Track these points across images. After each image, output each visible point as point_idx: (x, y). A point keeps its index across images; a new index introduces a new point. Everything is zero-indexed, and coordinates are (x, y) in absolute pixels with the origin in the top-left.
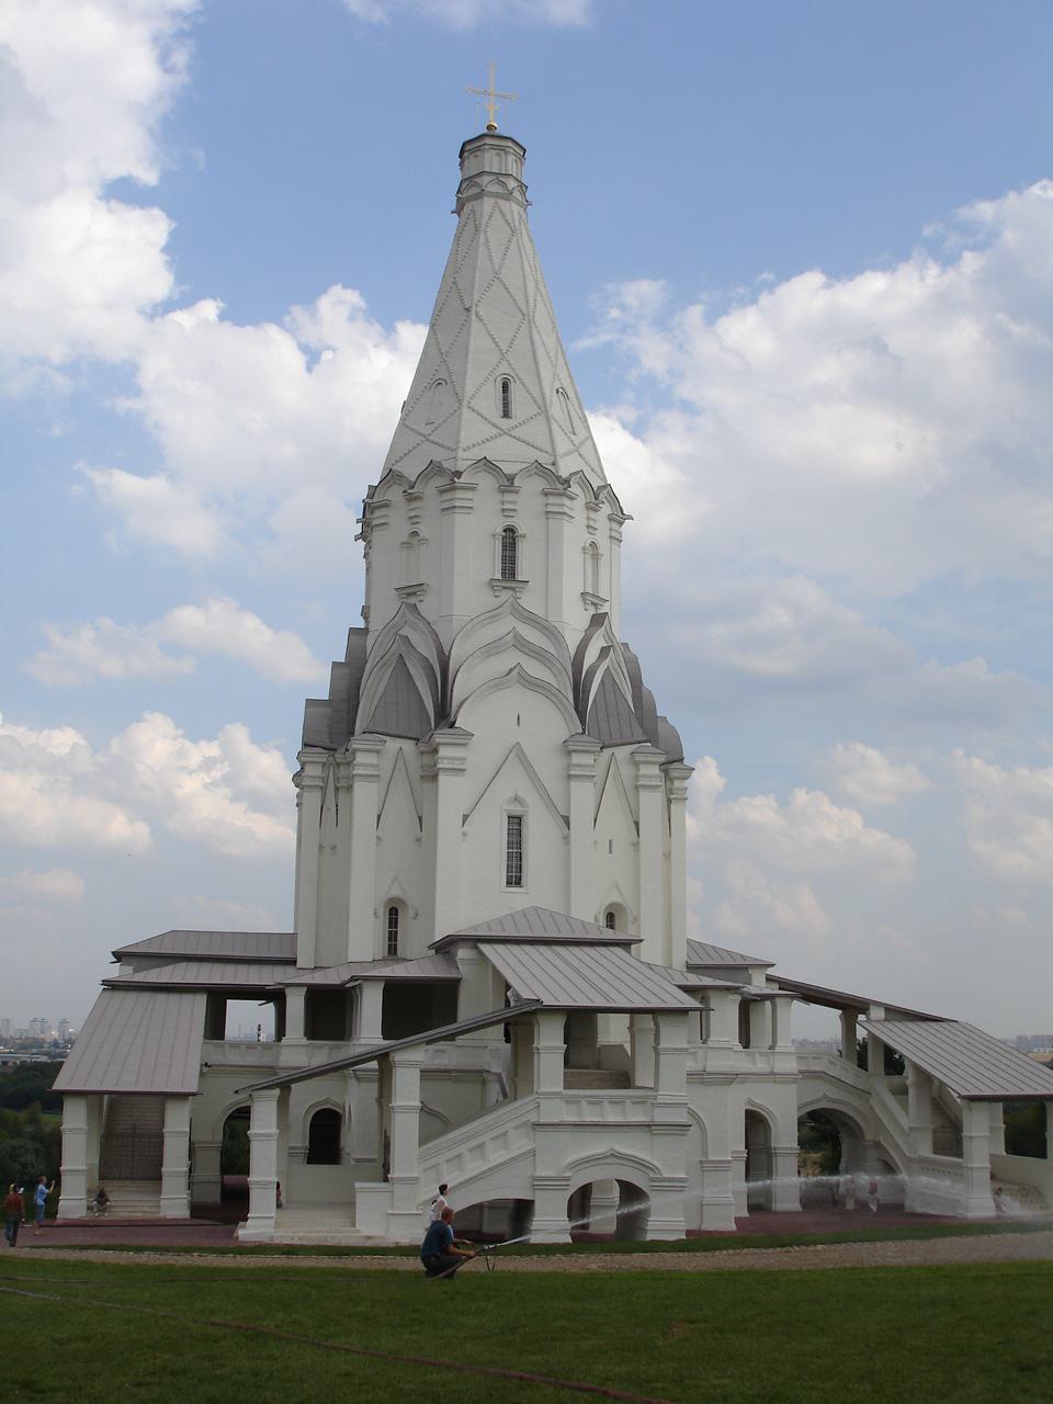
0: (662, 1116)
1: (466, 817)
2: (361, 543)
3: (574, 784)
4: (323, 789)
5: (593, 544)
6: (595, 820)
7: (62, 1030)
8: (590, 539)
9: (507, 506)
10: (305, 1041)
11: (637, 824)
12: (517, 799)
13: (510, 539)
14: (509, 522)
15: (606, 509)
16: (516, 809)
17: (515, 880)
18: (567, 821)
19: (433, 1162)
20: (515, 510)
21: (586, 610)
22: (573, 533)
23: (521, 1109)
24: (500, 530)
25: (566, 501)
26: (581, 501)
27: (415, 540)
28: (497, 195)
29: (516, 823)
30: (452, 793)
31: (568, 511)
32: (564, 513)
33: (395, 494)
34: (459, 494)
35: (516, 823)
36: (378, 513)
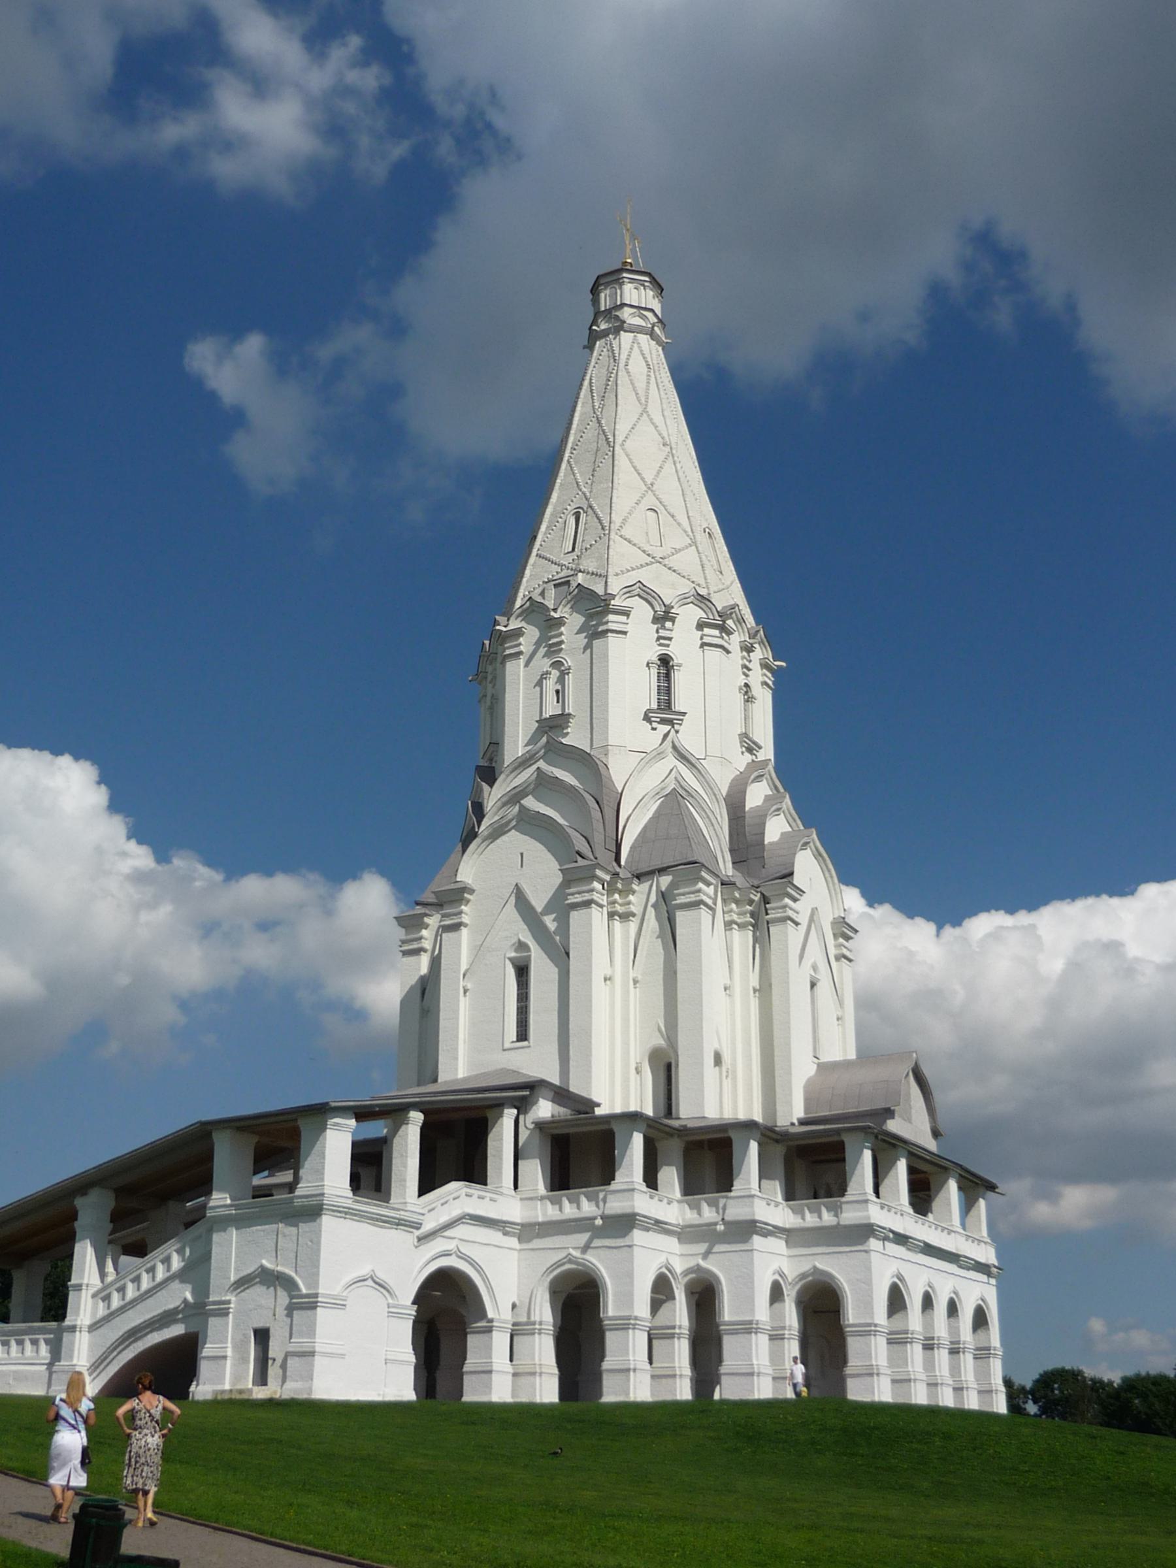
5: (665, 661)
12: (522, 946)
15: (688, 615)
25: (611, 617)
26: (642, 612)
29: (522, 972)
31: (611, 626)
35: (522, 972)
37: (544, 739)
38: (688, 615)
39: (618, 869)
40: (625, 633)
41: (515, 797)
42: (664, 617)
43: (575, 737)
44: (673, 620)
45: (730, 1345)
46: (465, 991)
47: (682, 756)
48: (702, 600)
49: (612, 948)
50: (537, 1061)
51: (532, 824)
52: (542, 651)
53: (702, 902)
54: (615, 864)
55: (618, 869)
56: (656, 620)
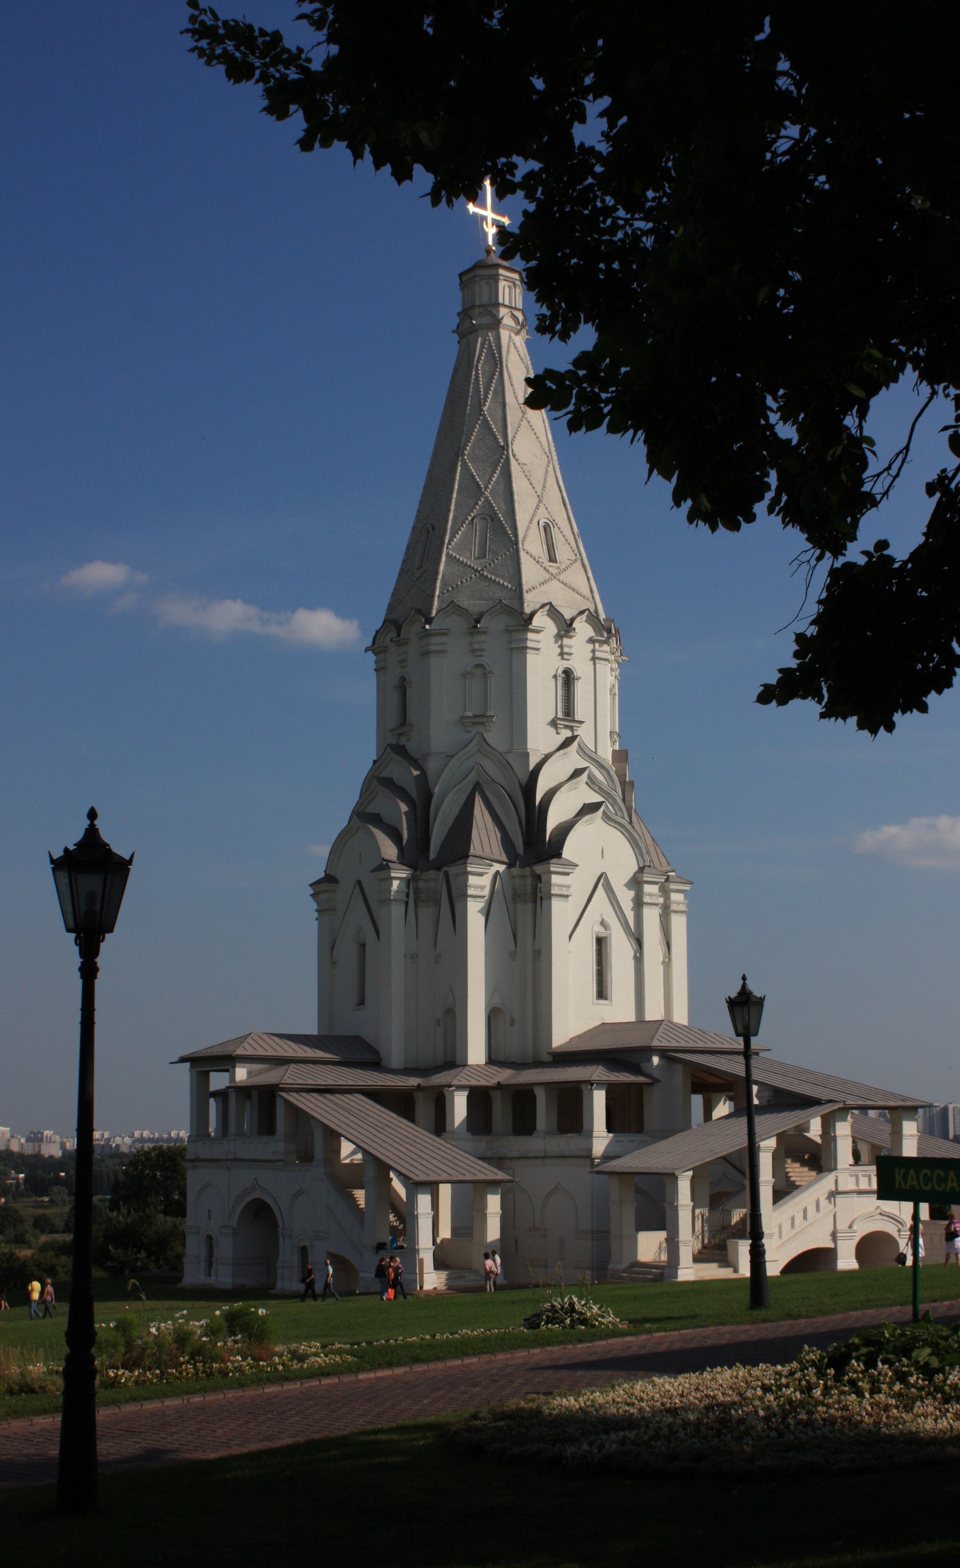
1: (570, 937)
2: (371, 657)
4: (407, 904)
9: (566, 650)
10: (469, 1135)
12: (603, 923)
13: (568, 678)
14: (566, 664)
17: (602, 993)
20: (570, 654)
23: (827, 1182)
24: (560, 671)
27: (479, 672)
28: (510, 329)
30: (561, 914)
33: (457, 624)
34: (530, 636)
36: (434, 640)
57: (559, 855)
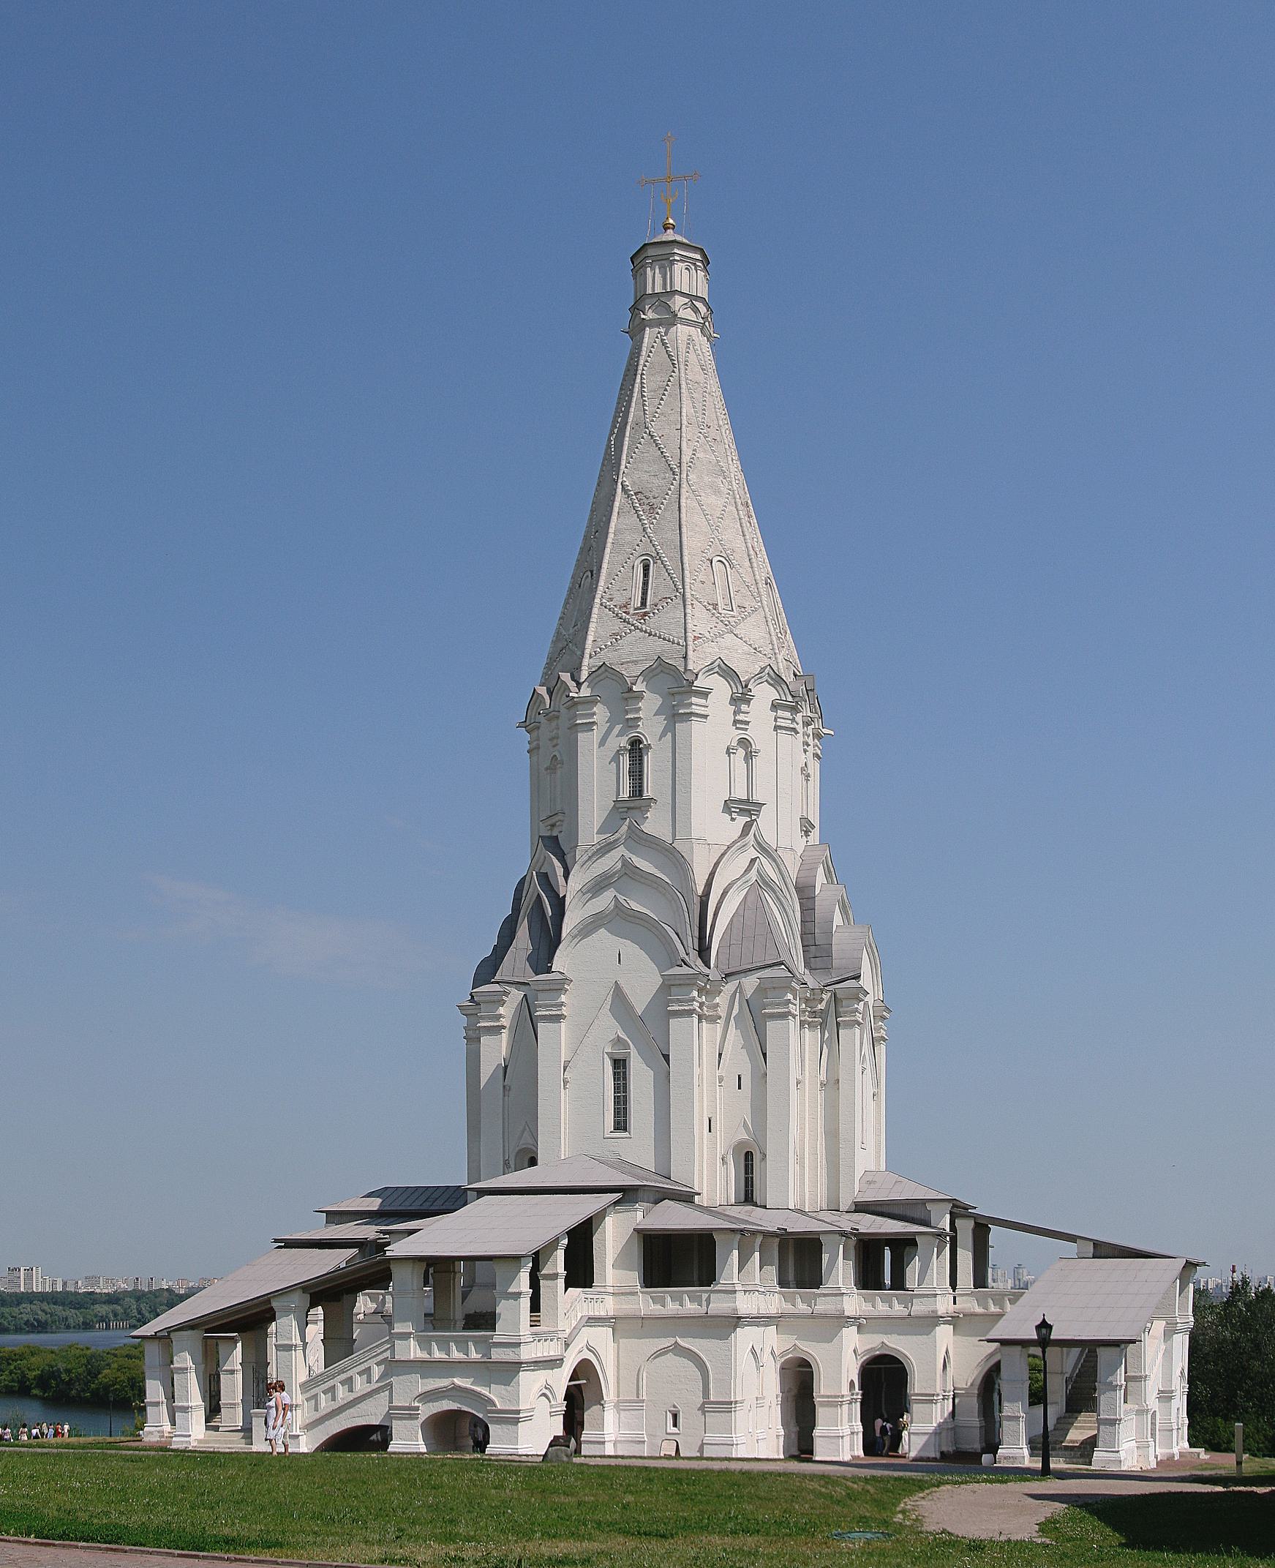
0: (497, 1355)
3: (674, 1022)
5: (744, 743)
6: (720, 1055)
7: (150, 1285)
8: (737, 734)
11: (765, 1055)
13: (637, 749)
15: (764, 694)
16: (620, 1053)
17: (621, 1124)
18: (666, 1057)
19: (313, 1392)
21: (733, 819)
22: (711, 730)
29: (620, 1066)
32: (692, 714)
35: (620, 1066)
37: (625, 828)
38: (764, 694)
39: (706, 970)
40: (706, 717)
41: (597, 887)
42: (741, 699)
43: (655, 824)
44: (748, 702)
45: (821, 1413)
46: (565, 1082)
47: (762, 848)
48: (777, 680)
49: (707, 1050)
50: (638, 1150)
51: (620, 920)
52: (618, 727)
53: (789, 1013)
54: (699, 962)
55: (706, 970)
56: (734, 701)
57: (549, 971)
